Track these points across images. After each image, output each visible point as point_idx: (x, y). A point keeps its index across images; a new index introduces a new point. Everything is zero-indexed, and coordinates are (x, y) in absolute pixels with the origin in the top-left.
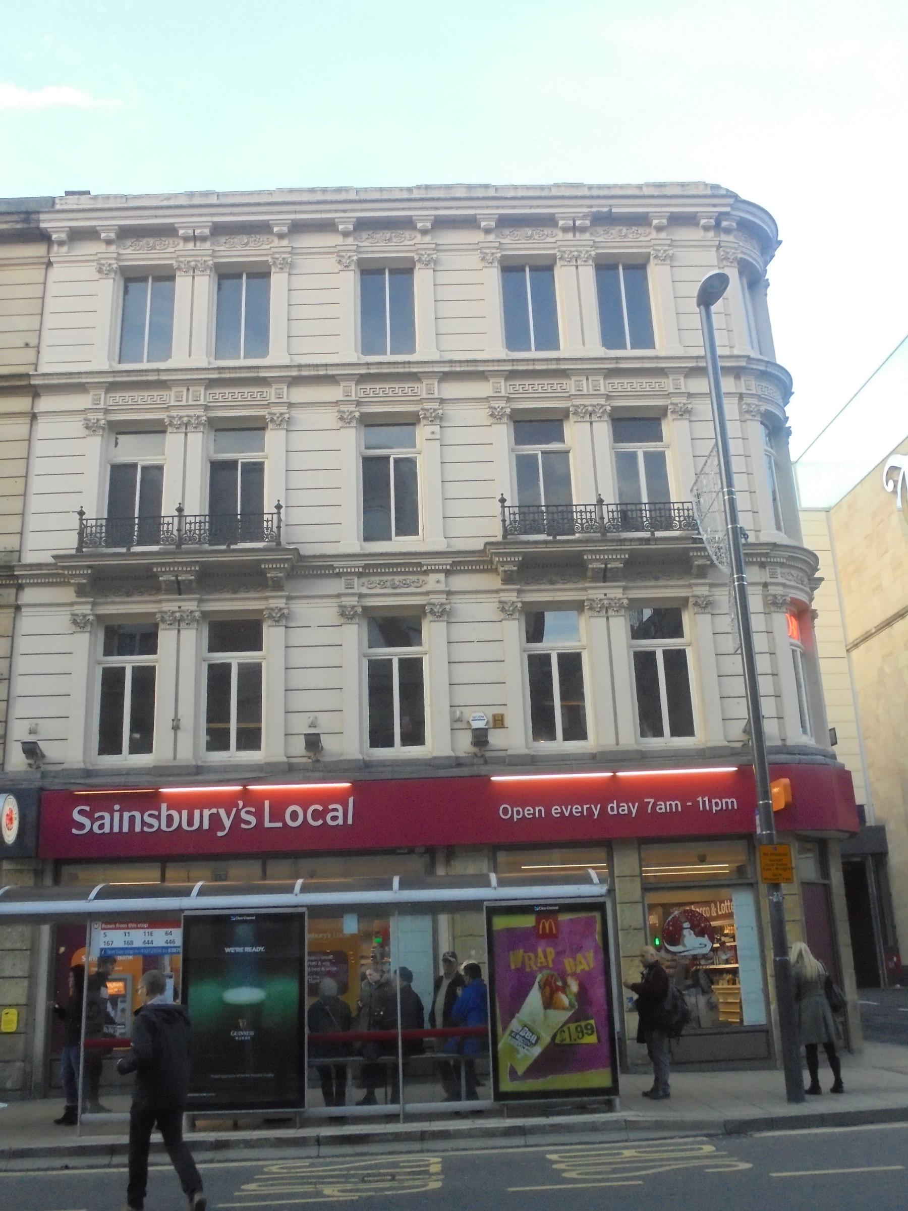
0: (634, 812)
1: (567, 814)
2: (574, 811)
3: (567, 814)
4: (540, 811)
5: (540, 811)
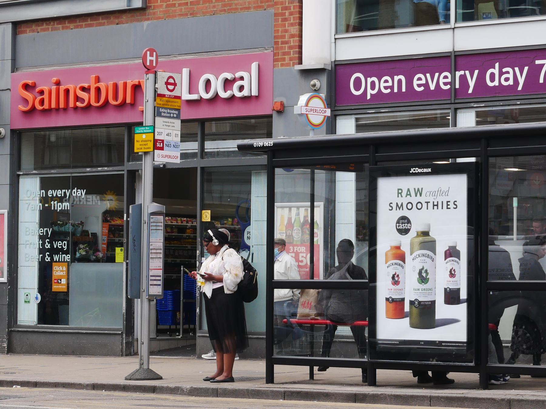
0: (521, 81)
1: (432, 87)
2: (442, 81)
3: (432, 87)
4: (400, 81)
5: (400, 81)
